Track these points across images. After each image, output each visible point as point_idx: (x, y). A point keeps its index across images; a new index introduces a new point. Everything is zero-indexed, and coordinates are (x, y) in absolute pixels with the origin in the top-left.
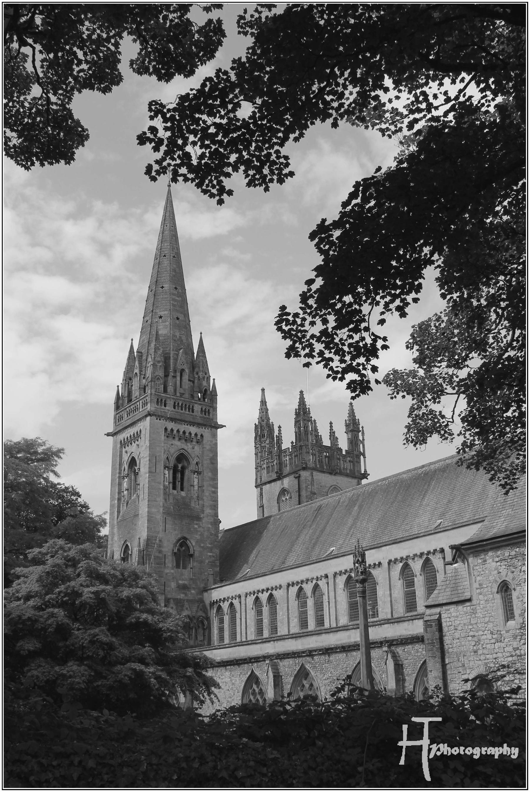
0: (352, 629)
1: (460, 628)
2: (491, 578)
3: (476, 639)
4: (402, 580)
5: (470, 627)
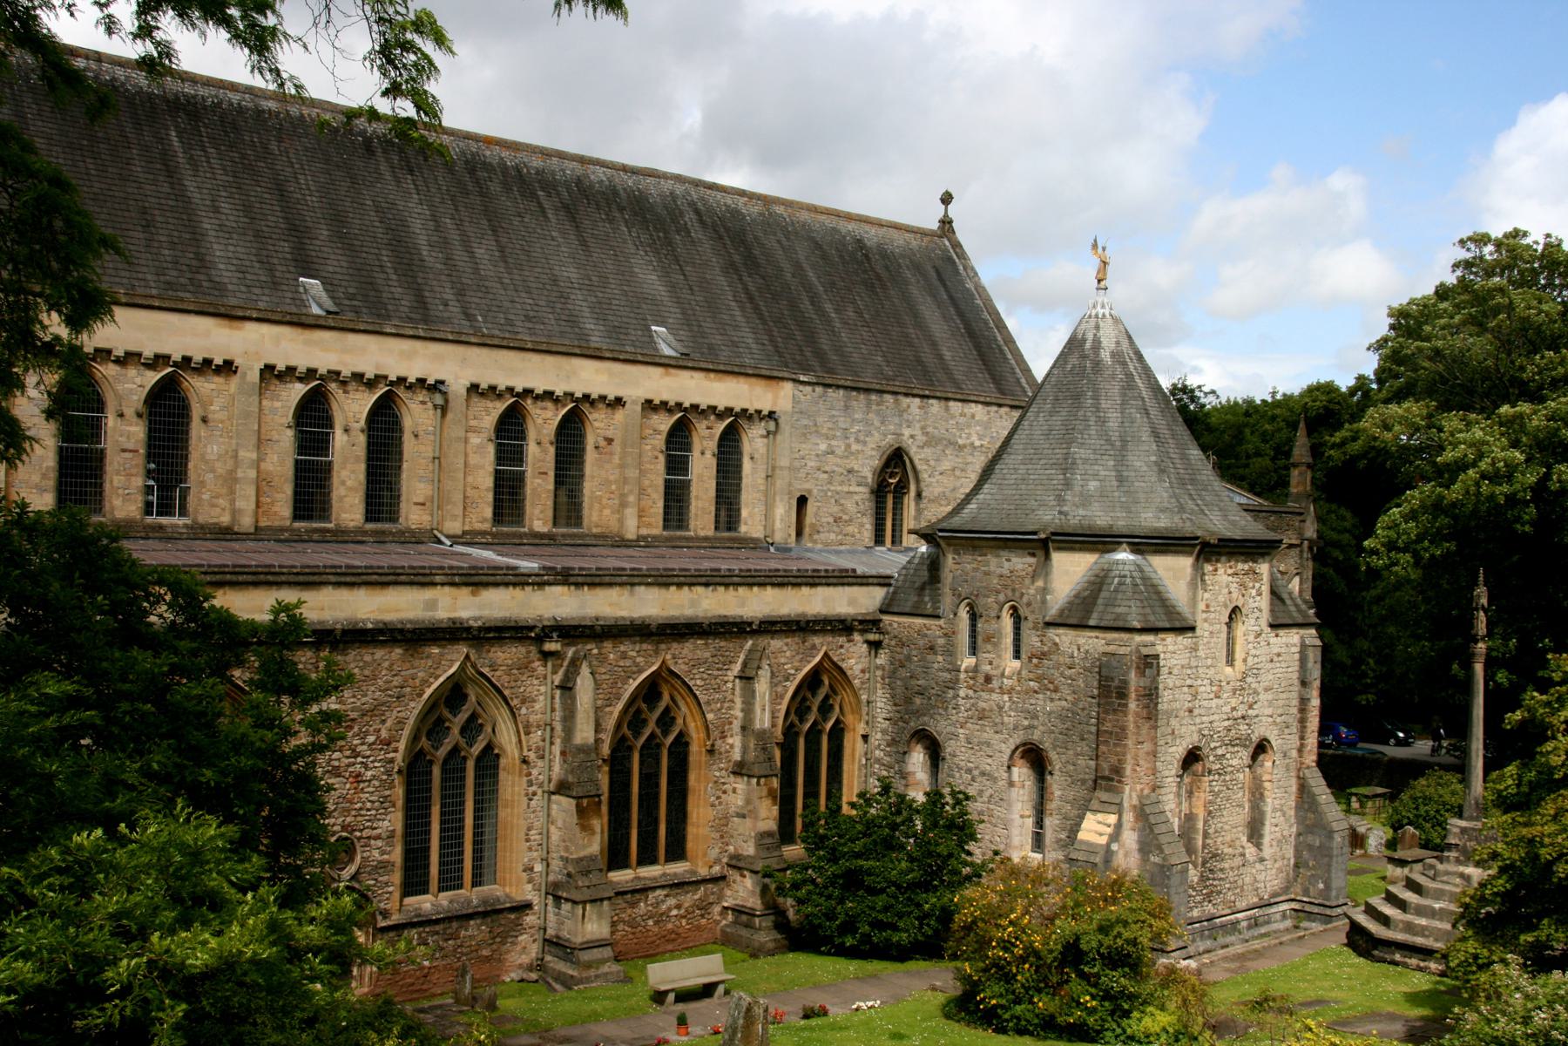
0: (443, 584)
1: (1175, 671)
2: (1221, 599)
3: (1192, 690)
4: (290, 433)
5: (1189, 672)
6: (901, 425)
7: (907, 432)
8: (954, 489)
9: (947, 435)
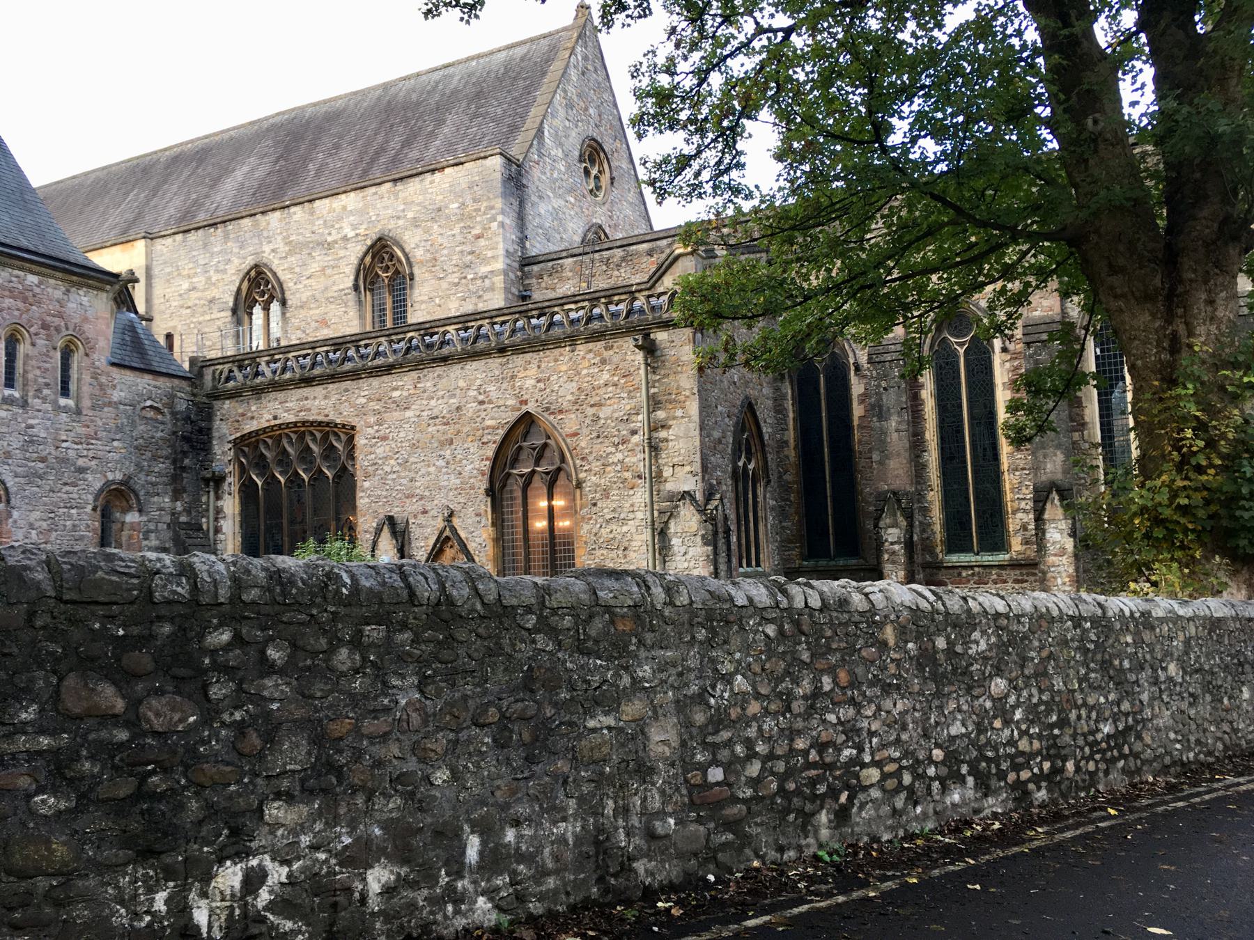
6: (261, 244)
7: (267, 248)
8: (326, 289)
9: (315, 237)
